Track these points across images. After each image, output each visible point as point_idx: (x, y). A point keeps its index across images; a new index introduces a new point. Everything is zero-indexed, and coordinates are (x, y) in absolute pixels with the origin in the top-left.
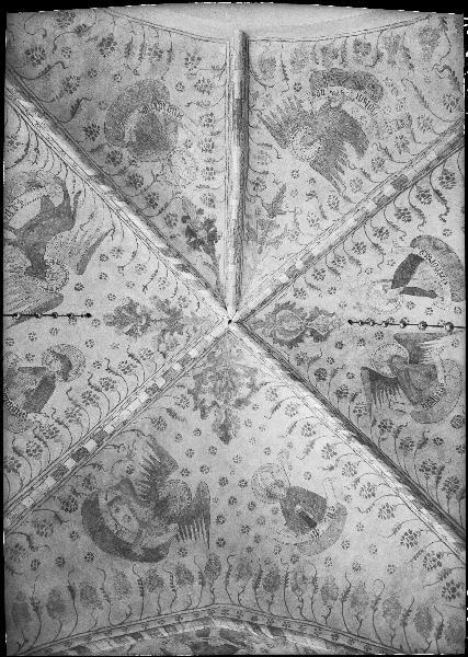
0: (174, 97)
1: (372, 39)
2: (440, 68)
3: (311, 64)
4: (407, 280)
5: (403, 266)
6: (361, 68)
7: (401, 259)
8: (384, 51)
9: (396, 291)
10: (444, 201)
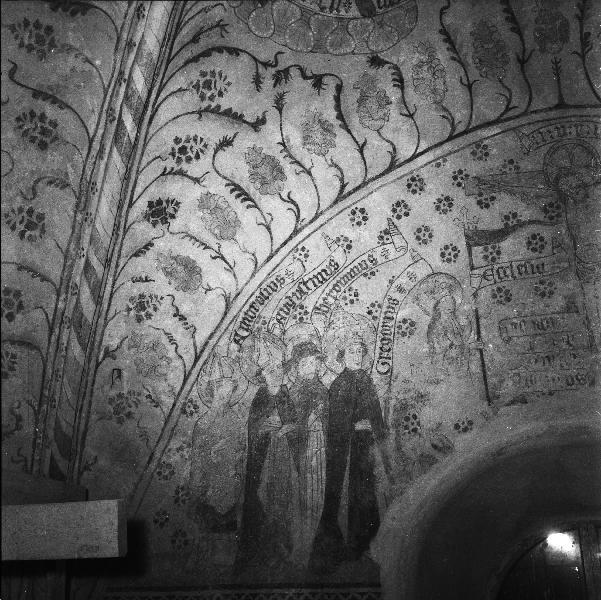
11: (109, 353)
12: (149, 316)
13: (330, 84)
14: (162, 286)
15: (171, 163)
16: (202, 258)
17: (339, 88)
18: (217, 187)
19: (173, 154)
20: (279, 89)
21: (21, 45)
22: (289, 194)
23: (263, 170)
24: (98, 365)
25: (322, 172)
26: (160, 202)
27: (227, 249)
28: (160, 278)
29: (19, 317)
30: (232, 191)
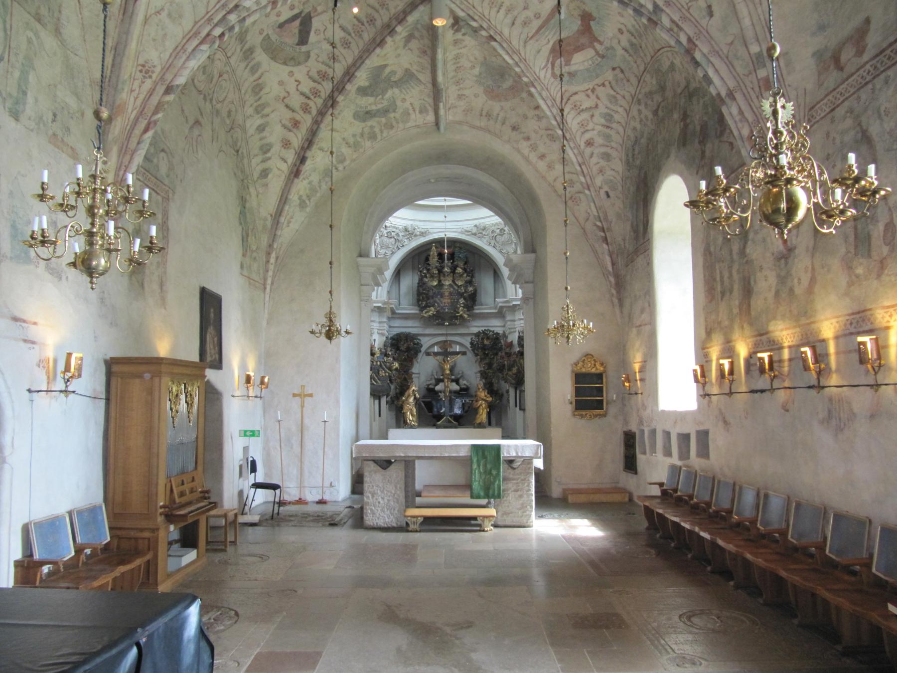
0: (480, 90)
1: (368, 144)
3: (397, 115)
4: (301, 24)
5: (308, 33)
6: (369, 123)
7: (313, 38)
9: (306, 11)
10: (302, 94)
11: (600, 188)
13: (607, 83)
14: (603, 163)
15: (582, 130)
16: (608, 150)
17: (610, 83)
18: (599, 128)
20: (595, 93)
23: (607, 117)
25: (620, 110)
27: (613, 144)
28: (601, 160)
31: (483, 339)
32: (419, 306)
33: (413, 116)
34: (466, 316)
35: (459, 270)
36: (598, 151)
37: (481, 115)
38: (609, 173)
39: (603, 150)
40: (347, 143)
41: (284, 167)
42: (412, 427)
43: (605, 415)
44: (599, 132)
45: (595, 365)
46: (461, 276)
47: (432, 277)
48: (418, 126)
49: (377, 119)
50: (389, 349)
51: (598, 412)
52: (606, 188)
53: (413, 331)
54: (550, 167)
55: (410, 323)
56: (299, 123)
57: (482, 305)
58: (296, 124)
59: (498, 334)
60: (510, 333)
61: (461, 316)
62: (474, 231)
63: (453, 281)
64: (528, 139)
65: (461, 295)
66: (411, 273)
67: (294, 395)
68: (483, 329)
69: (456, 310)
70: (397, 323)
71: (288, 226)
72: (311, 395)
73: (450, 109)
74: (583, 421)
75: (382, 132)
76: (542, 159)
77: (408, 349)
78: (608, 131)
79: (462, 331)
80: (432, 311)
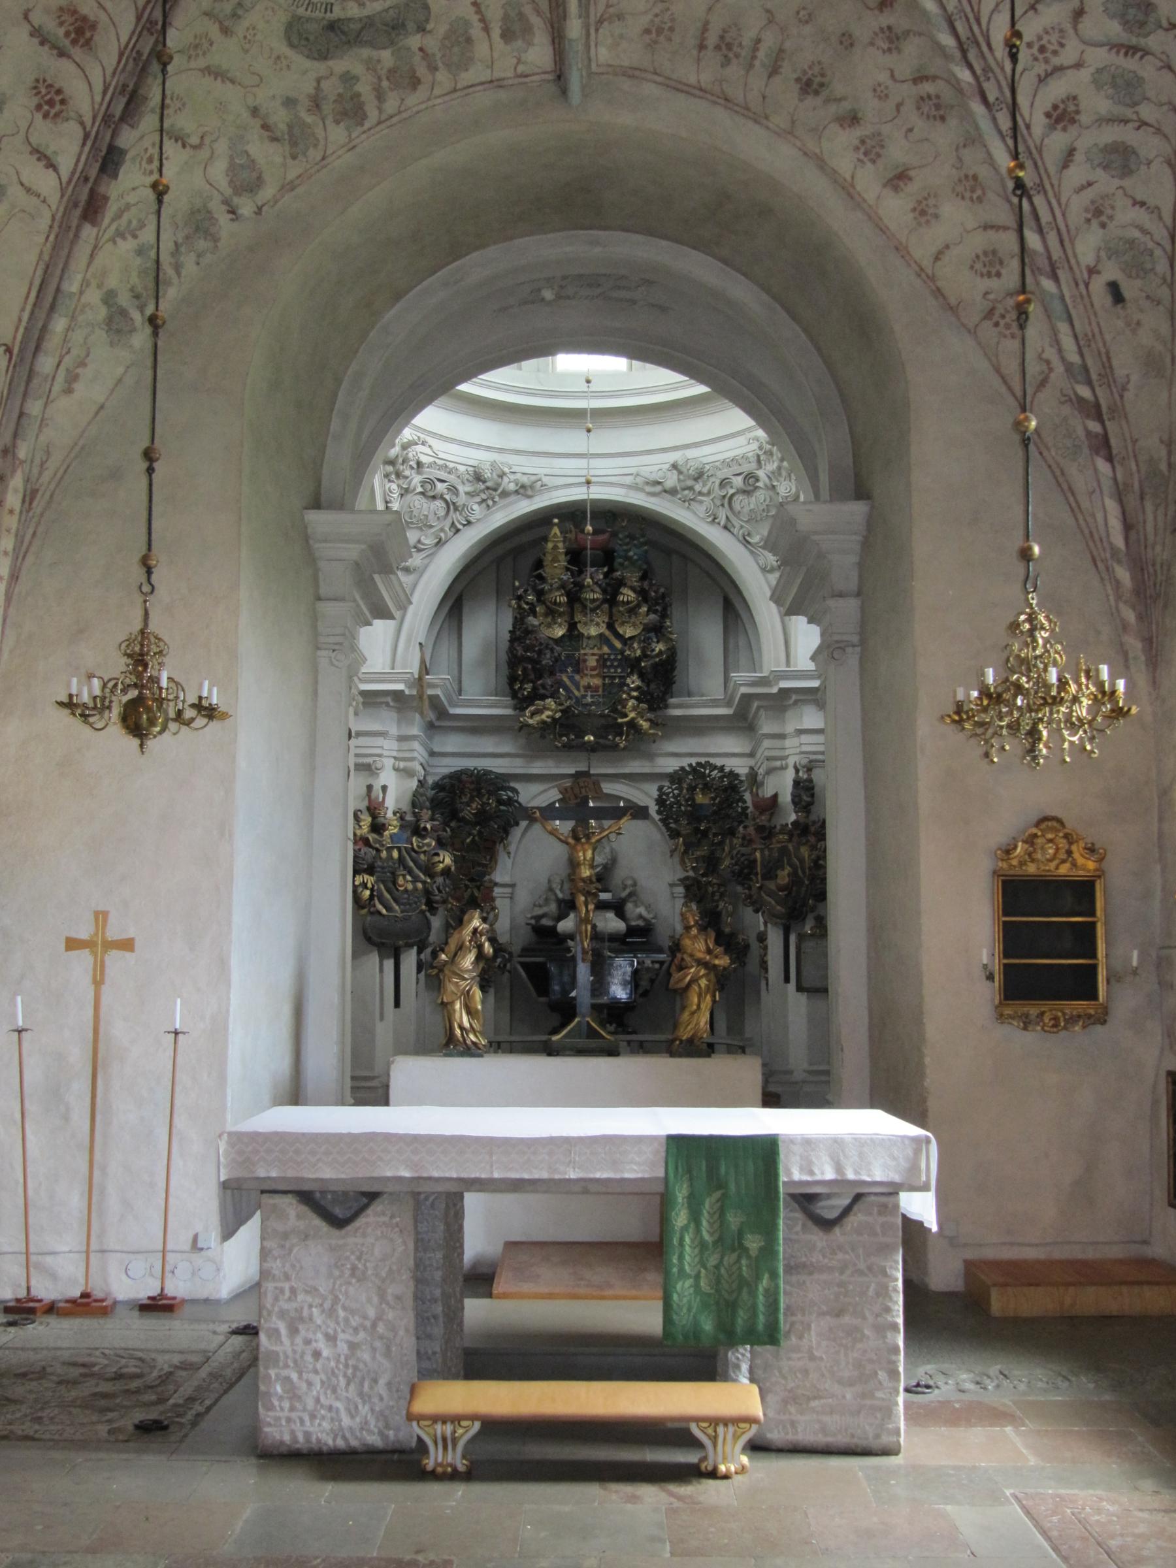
1: (337, 134)
2: (207, 140)
6: (340, 65)
8: (309, 119)
11: (1092, 271)
12: (1111, 218)
14: (1106, 182)
16: (1127, 135)
18: (1099, 57)
19: (1036, 59)
21: (884, 52)
22: (1168, 19)
24: (1087, 285)
26: (1055, 107)
27: (1147, 112)
28: (1100, 174)
29: (1003, 272)
30: (1118, 52)
31: (692, 789)
32: (514, 695)
33: (481, 49)
34: (645, 725)
35: (627, 595)
36: (1091, 139)
37: (702, 47)
38: (1126, 215)
39: (1110, 135)
40: (265, 127)
41: (47, 183)
42: (470, 1051)
43: (1101, 1018)
44: (1099, 71)
45: (1069, 853)
46: (633, 611)
47: (551, 612)
48: (496, 84)
49: (366, 52)
50: (426, 814)
51: (1079, 1006)
52: (1111, 272)
53: (499, 766)
54: (923, 213)
55: (488, 744)
56: (93, 27)
57: (689, 695)
58: (80, 31)
59: (733, 775)
60: (769, 772)
61: (632, 724)
62: (672, 481)
63: (611, 626)
64: (853, 119)
65: (633, 665)
66: (492, 606)
67: (72, 944)
68: (694, 761)
69: (617, 708)
70: (452, 743)
71: (69, 391)
72: (127, 945)
73: (600, 22)
74: (1031, 1038)
75: (380, 97)
76: (896, 189)
77: (482, 817)
78: (1130, 64)
79: (636, 766)
80: (549, 710)
